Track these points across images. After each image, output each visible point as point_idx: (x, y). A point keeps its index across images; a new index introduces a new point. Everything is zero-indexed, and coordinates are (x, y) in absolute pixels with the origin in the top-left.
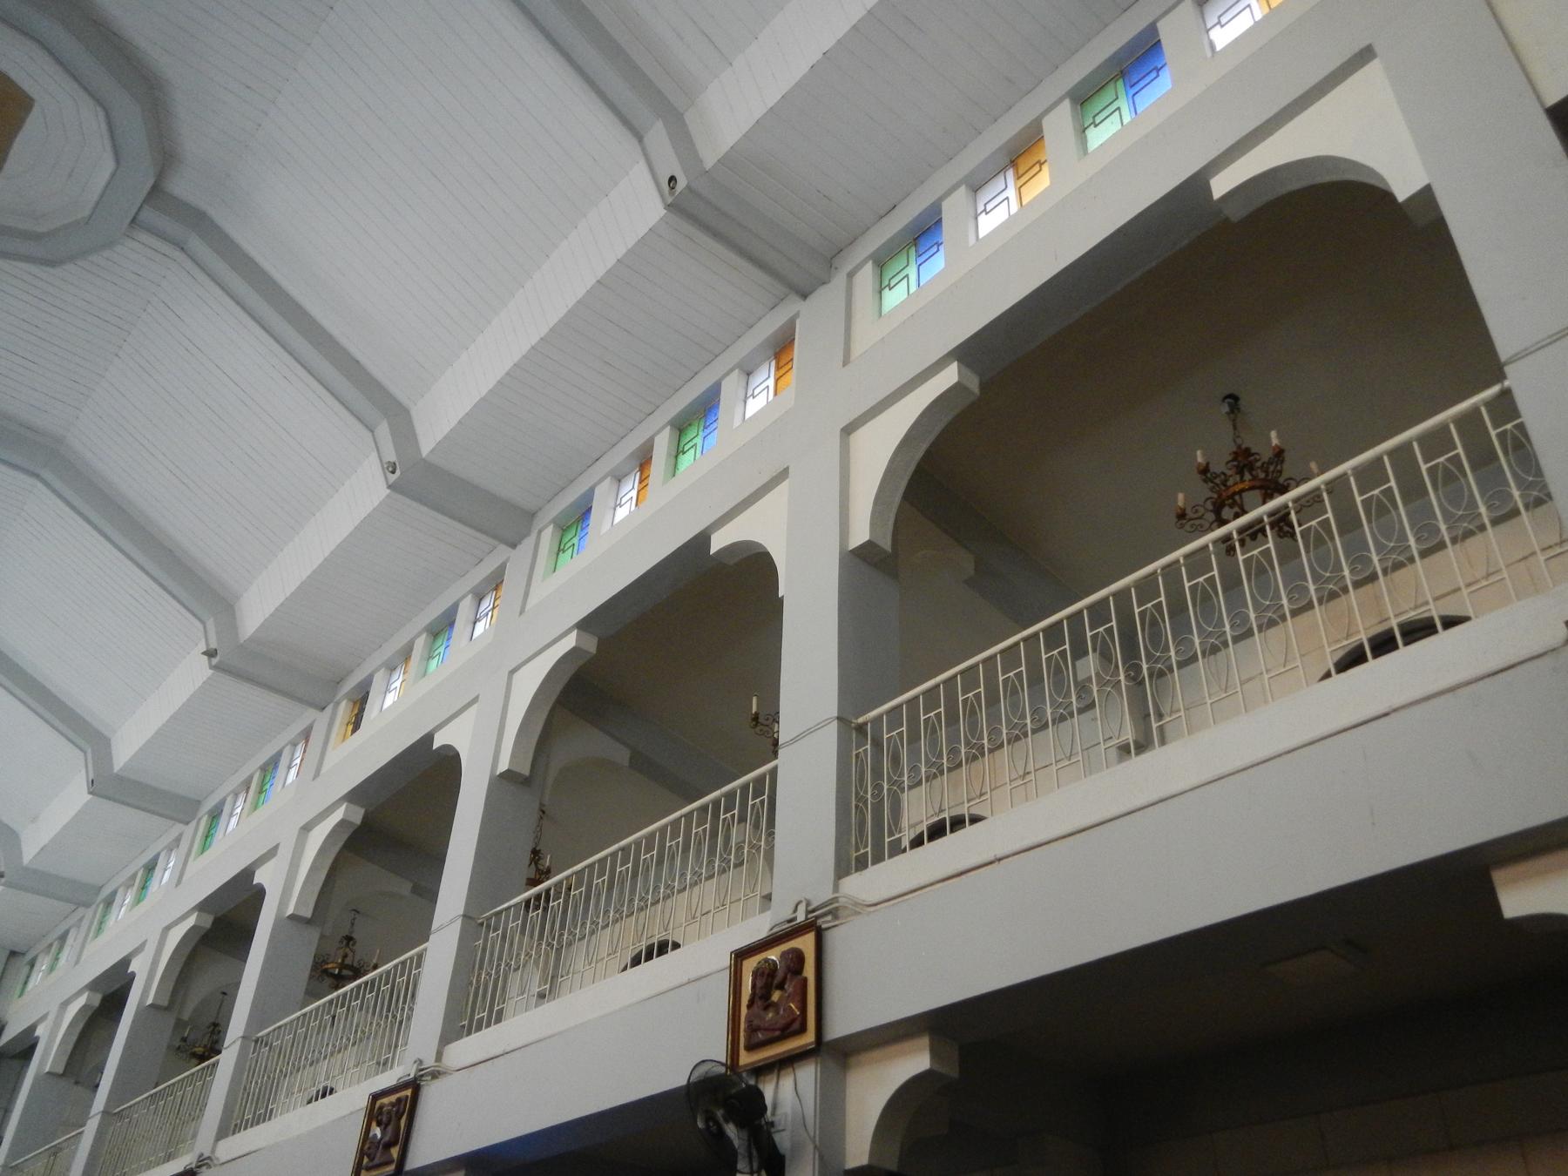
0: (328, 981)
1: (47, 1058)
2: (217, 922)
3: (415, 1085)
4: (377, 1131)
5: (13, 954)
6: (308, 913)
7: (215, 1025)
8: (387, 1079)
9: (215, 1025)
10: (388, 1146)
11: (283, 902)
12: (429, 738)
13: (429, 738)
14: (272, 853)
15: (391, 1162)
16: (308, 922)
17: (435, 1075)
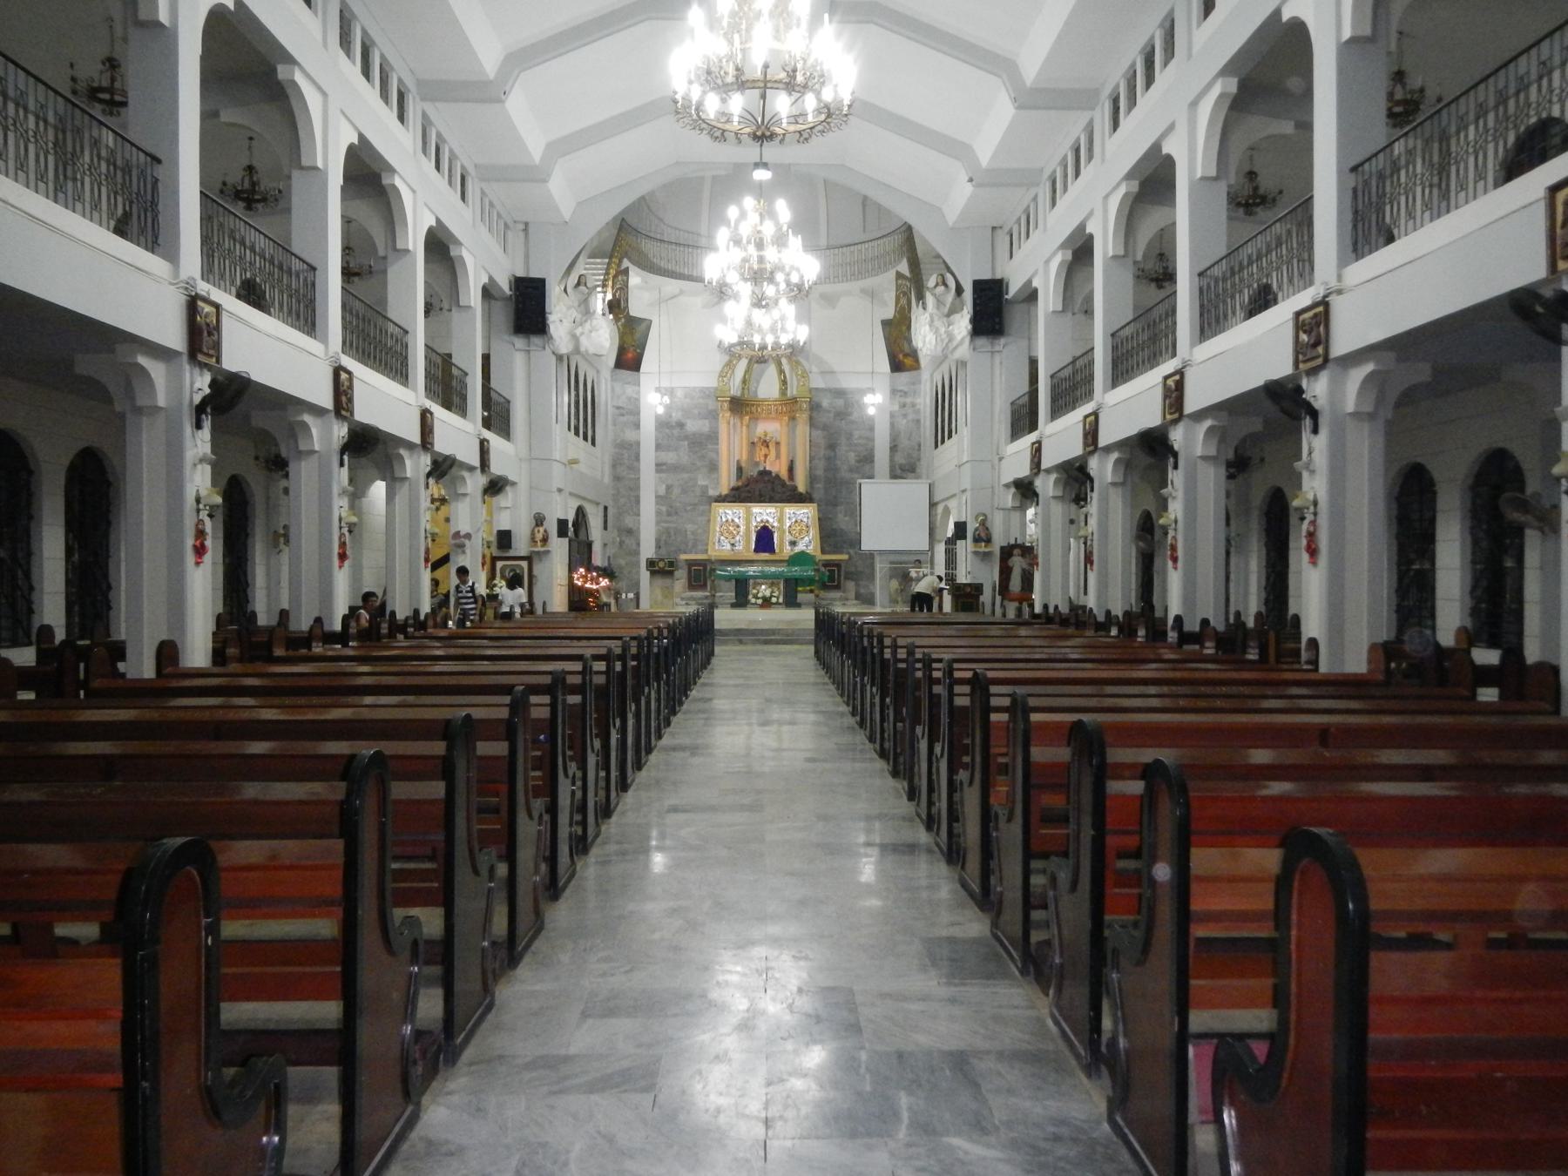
0: (1241, 210)
1: (1049, 300)
2: (1143, 185)
3: (1324, 303)
4: (1304, 337)
5: (994, 228)
6: (1214, 173)
7: (1161, 255)
8: (1304, 298)
9: (1161, 255)
10: (1315, 345)
11: (1192, 169)
12: (1277, 13)
13: (1277, 13)
14: (1172, 127)
15: (1317, 357)
16: (1216, 179)
17: (1339, 292)
